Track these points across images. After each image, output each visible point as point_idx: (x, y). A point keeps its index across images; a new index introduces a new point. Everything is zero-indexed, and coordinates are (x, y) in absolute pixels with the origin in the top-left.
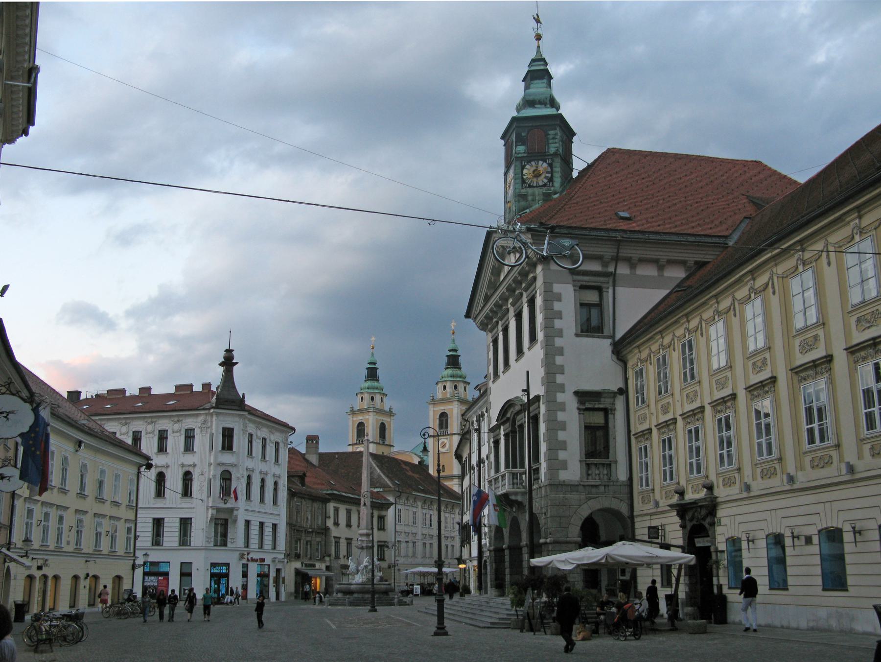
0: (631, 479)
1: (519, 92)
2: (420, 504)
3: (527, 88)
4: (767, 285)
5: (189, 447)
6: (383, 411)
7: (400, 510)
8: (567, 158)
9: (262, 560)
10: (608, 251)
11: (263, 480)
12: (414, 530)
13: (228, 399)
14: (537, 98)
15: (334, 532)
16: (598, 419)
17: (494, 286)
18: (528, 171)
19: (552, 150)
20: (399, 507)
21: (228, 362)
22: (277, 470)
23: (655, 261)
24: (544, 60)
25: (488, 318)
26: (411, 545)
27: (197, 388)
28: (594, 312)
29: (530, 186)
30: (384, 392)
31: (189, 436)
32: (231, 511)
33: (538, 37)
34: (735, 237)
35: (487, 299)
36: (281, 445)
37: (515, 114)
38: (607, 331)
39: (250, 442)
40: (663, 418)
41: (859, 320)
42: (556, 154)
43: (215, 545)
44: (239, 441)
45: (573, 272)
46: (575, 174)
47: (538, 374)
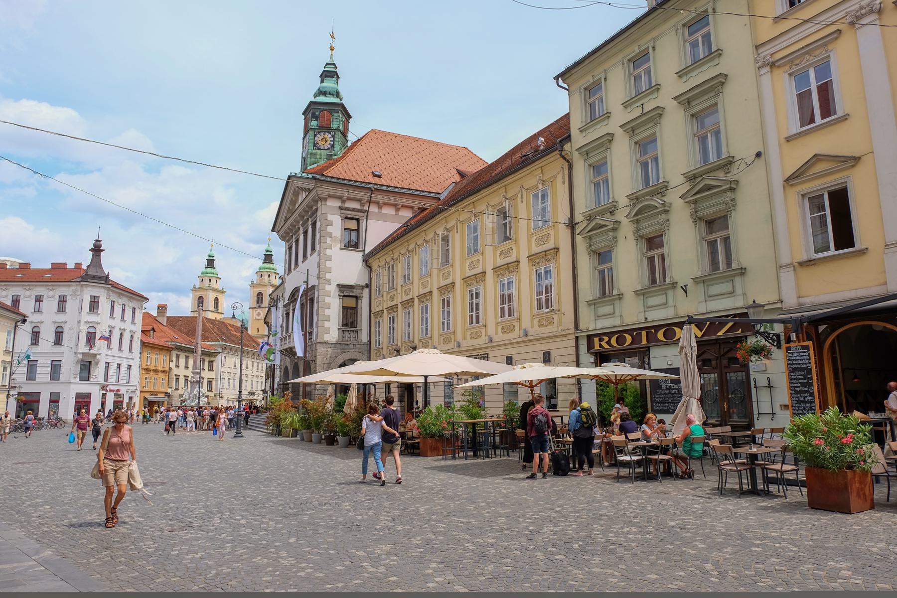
0: (370, 341)
1: (316, 84)
3: (322, 82)
4: (453, 226)
8: (344, 135)
9: (118, 391)
10: (364, 196)
11: (121, 334)
12: (235, 371)
13: (93, 275)
14: (328, 91)
16: (351, 303)
17: (291, 212)
18: (319, 137)
19: (335, 126)
22: (133, 328)
23: (395, 205)
24: (334, 64)
25: (287, 233)
27: (71, 266)
28: (354, 234)
29: (319, 149)
31: (62, 301)
32: (95, 355)
33: (332, 49)
34: (445, 194)
35: (286, 220)
37: (313, 99)
38: (361, 248)
39: (113, 307)
40: (390, 304)
41: (502, 252)
42: (338, 129)
44: (104, 305)
45: (340, 208)
46: (349, 144)
47: (314, 272)
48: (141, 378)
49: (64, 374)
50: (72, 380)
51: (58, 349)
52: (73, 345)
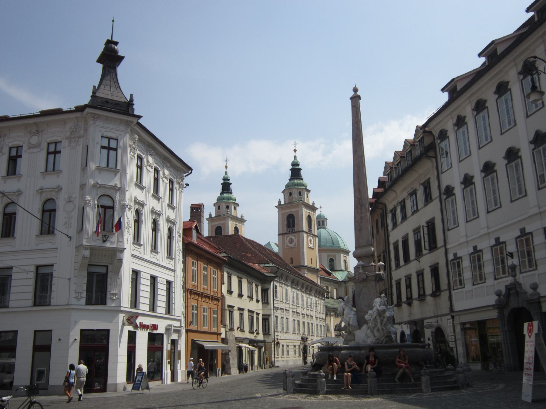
2: (290, 282)
5: (52, 169)
6: (237, 217)
7: (276, 286)
9: (155, 327)
12: (287, 306)
15: (230, 300)
20: (276, 284)
21: (110, 58)
30: (236, 202)
39: (140, 167)
43: (89, 302)
48: (186, 307)
50: (73, 301)
52: (72, 232)
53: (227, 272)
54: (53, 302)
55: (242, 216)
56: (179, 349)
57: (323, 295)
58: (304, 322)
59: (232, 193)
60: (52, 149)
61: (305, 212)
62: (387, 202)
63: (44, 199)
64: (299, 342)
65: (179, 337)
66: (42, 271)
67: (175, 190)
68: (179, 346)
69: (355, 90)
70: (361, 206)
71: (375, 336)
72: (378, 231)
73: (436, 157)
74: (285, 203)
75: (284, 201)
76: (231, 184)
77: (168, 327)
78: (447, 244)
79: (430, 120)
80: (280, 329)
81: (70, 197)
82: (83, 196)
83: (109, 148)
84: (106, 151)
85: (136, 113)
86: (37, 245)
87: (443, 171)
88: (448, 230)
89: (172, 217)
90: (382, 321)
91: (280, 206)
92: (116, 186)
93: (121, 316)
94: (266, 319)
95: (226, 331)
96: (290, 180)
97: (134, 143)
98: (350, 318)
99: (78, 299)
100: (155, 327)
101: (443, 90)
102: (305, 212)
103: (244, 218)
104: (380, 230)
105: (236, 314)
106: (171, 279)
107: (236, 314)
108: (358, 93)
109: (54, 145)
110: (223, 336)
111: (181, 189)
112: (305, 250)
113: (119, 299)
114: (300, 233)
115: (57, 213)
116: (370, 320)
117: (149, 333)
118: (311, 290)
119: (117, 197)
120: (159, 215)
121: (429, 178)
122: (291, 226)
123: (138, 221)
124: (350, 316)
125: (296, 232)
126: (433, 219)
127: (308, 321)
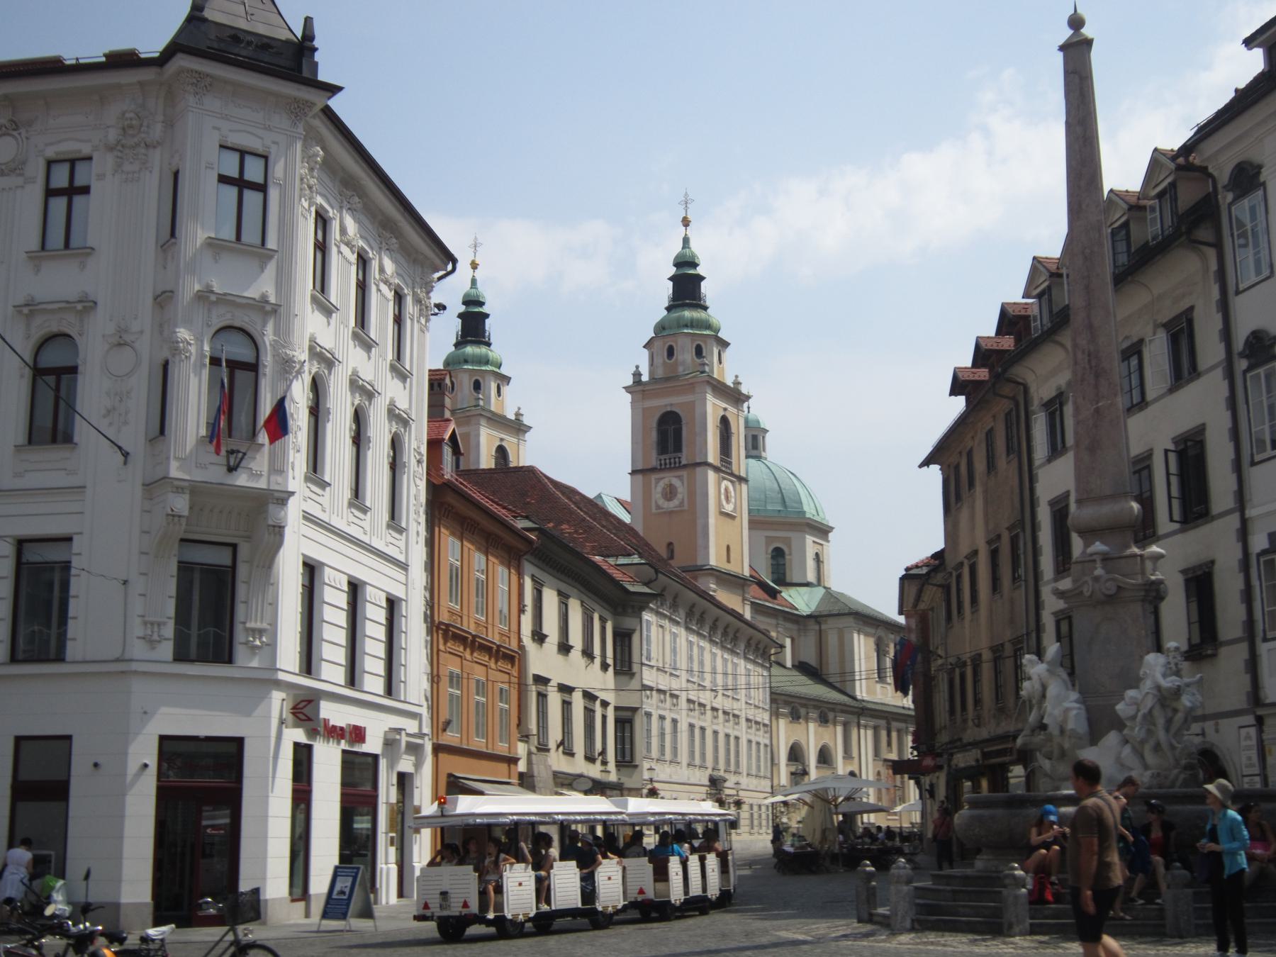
2: (682, 613)
6: (504, 417)
9: (358, 734)
11: (359, 417)
12: (674, 684)
26: (668, 725)
30: (504, 371)
36: (410, 307)
39: (322, 247)
43: (181, 655)
48: (435, 679)
49: (93, 617)
50: (138, 649)
51: (49, 467)
52: (134, 435)
53: (533, 578)
54: (72, 650)
55: (518, 414)
56: (416, 803)
57: (765, 655)
58: (716, 733)
59: (488, 344)
60: (60, 178)
61: (713, 407)
62: (1030, 379)
63: (37, 334)
64: (704, 789)
65: (418, 765)
66: (34, 555)
67: (408, 322)
68: (416, 792)
69: (1076, 22)
70: (1097, 376)
71: (1146, 767)
72: (991, 465)
73: (1218, 246)
74: (653, 379)
75: (651, 373)
76: (487, 316)
77: (391, 736)
78: (1248, 506)
79: (1207, 131)
80: (655, 753)
81: (122, 331)
82: (163, 328)
83: (241, 184)
84: (232, 192)
85: (323, 76)
86: (18, 475)
87: (1241, 287)
88: (1253, 464)
89: (402, 404)
90: (1169, 722)
91: (637, 388)
92: (264, 300)
93: (277, 697)
94: (625, 720)
95: (530, 754)
96: (669, 309)
97: (311, 169)
98: (1067, 710)
99: (151, 643)
100: (358, 734)
101: (1249, 42)
102: (713, 407)
103: (526, 421)
104: (1002, 462)
105: (554, 700)
106: (398, 592)
107: (554, 700)
108: (1087, 31)
109: (66, 167)
110: (522, 767)
111: (423, 321)
112: (712, 520)
113: (272, 646)
114: (699, 470)
115: (80, 377)
116: (1134, 718)
117: (344, 752)
118: (735, 639)
119: (268, 336)
120: (370, 394)
121: (1191, 308)
122: (671, 447)
123: (317, 412)
124: (1067, 705)
125: (685, 466)
126: (1201, 429)
127: (728, 731)
